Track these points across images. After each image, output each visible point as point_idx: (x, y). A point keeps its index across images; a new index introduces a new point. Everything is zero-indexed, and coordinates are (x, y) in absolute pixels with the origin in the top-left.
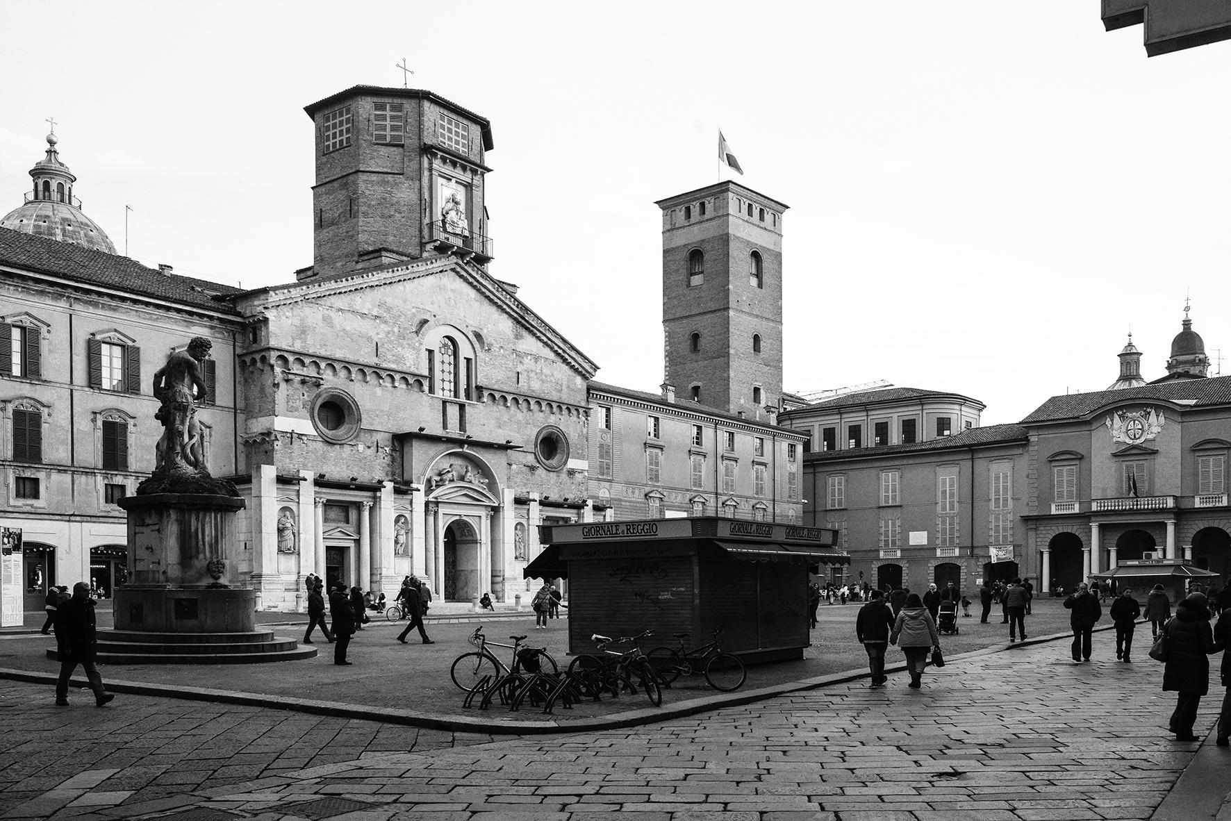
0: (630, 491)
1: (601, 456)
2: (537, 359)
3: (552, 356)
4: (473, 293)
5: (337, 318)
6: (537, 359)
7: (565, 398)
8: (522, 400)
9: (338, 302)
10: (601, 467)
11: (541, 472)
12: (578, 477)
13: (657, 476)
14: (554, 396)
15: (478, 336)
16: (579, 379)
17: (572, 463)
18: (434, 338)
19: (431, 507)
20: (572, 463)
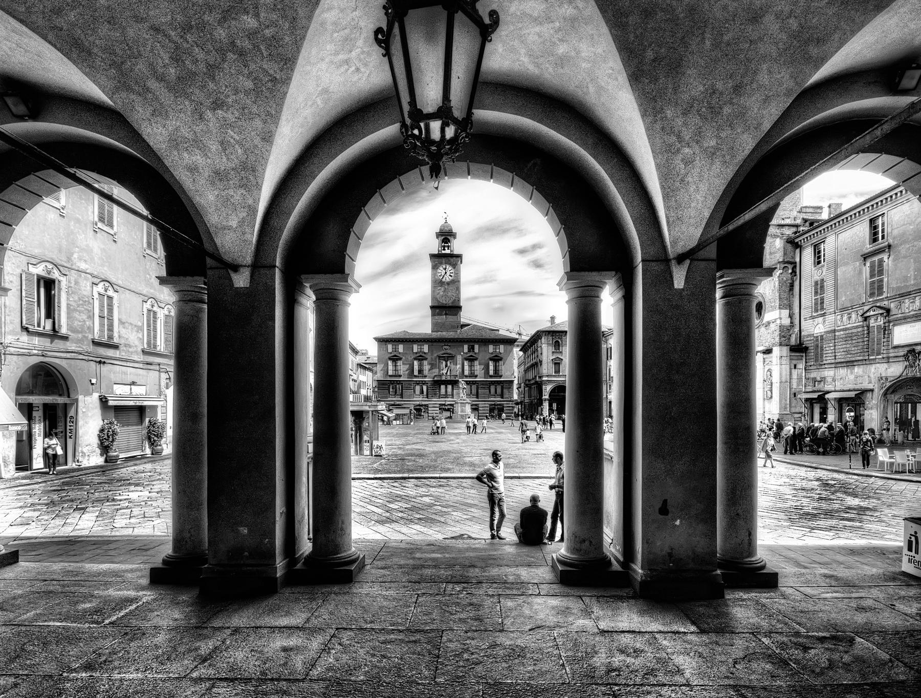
0: (845, 318)
1: (816, 293)
10: (816, 304)
12: (772, 325)
13: (880, 288)
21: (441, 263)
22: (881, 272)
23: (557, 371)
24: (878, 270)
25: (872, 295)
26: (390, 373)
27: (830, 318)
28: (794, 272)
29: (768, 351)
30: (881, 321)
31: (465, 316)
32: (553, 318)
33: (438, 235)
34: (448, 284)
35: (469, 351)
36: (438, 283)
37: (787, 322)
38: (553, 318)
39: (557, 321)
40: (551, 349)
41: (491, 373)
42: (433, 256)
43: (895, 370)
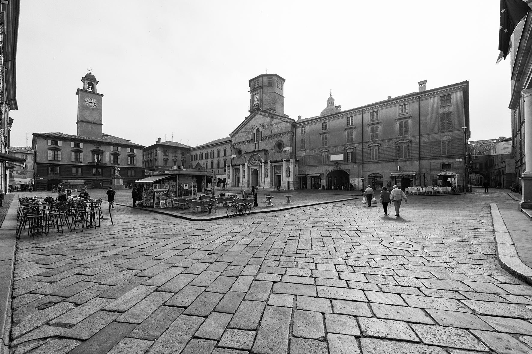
2: (276, 124)
3: (280, 121)
4: (261, 116)
5: (240, 135)
6: (276, 124)
7: (284, 131)
8: (270, 137)
9: (240, 132)
11: (276, 154)
13: (326, 144)
14: (281, 132)
15: (263, 126)
16: (288, 124)
17: (285, 149)
18: (255, 131)
19: (249, 167)
20: (285, 149)
21: (88, 96)
22: (326, 139)
23: (166, 164)
24: (325, 138)
25: (323, 145)
26: (50, 158)
27: (308, 151)
28: (293, 136)
29: (288, 161)
30: (326, 154)
31: (105, 130)
32: (159, 139)
33: (83, 79)
34: (93, 109)
35: (131, 151)
36: (82, 107)
37: (292, 151)
38: (159, 139)
39: (162, 141)
40: (163, 154)
41: (129, 163)
42: (79, 90)
43: (331, 168)
